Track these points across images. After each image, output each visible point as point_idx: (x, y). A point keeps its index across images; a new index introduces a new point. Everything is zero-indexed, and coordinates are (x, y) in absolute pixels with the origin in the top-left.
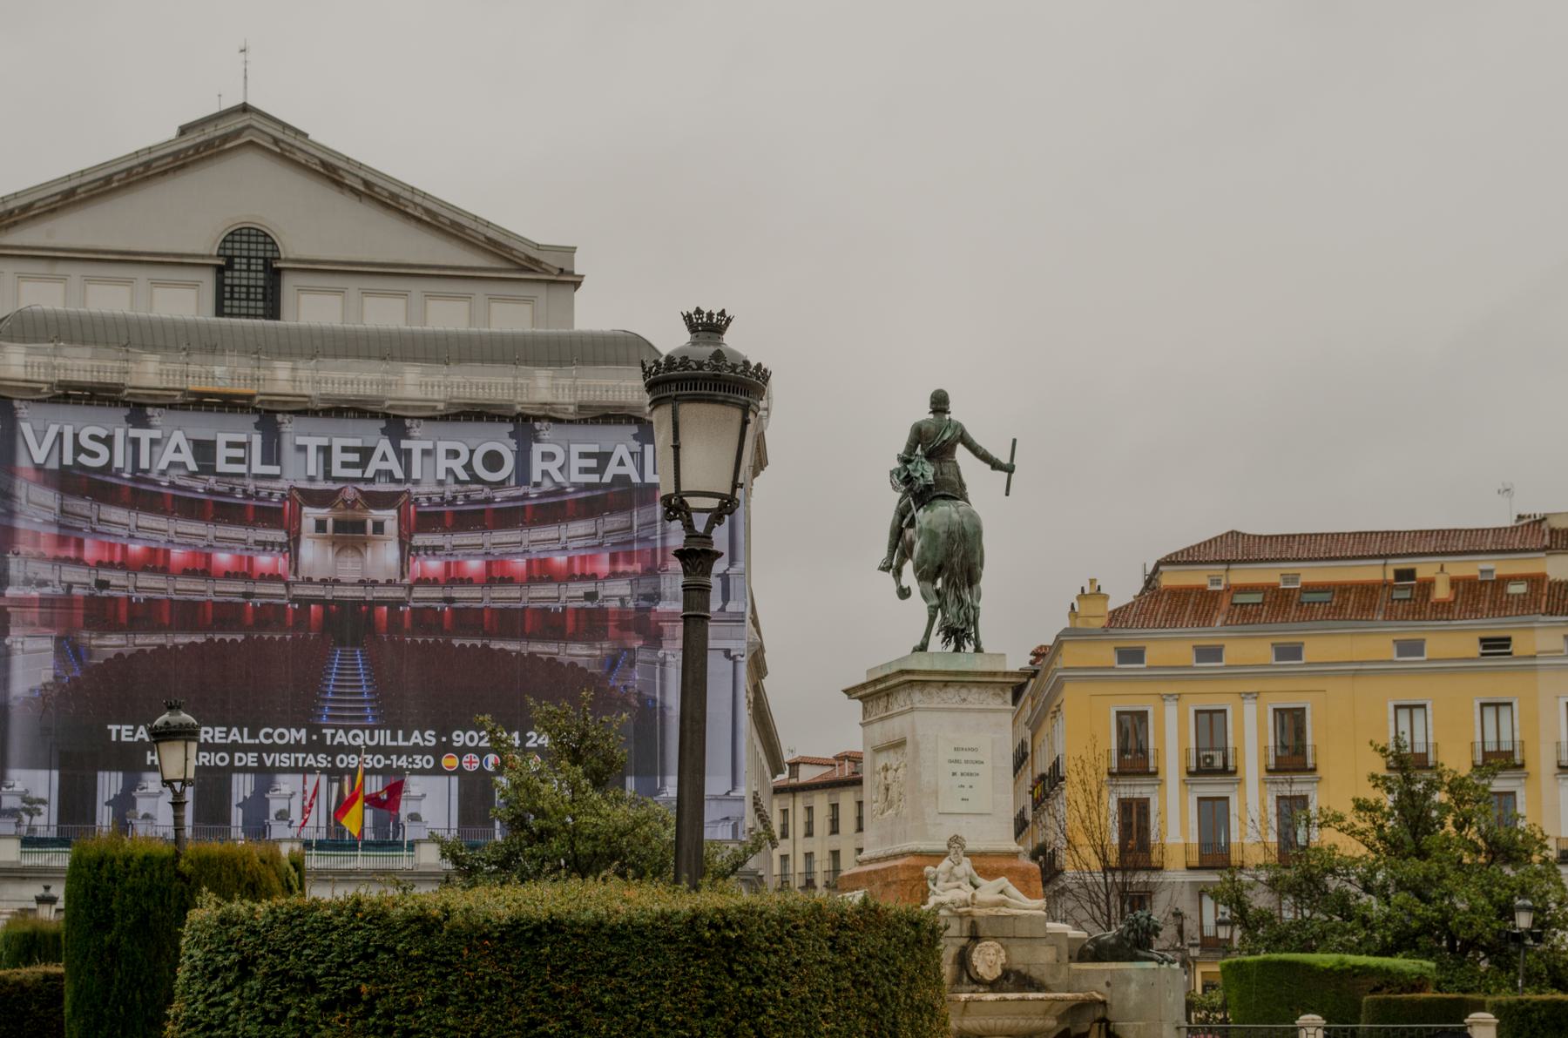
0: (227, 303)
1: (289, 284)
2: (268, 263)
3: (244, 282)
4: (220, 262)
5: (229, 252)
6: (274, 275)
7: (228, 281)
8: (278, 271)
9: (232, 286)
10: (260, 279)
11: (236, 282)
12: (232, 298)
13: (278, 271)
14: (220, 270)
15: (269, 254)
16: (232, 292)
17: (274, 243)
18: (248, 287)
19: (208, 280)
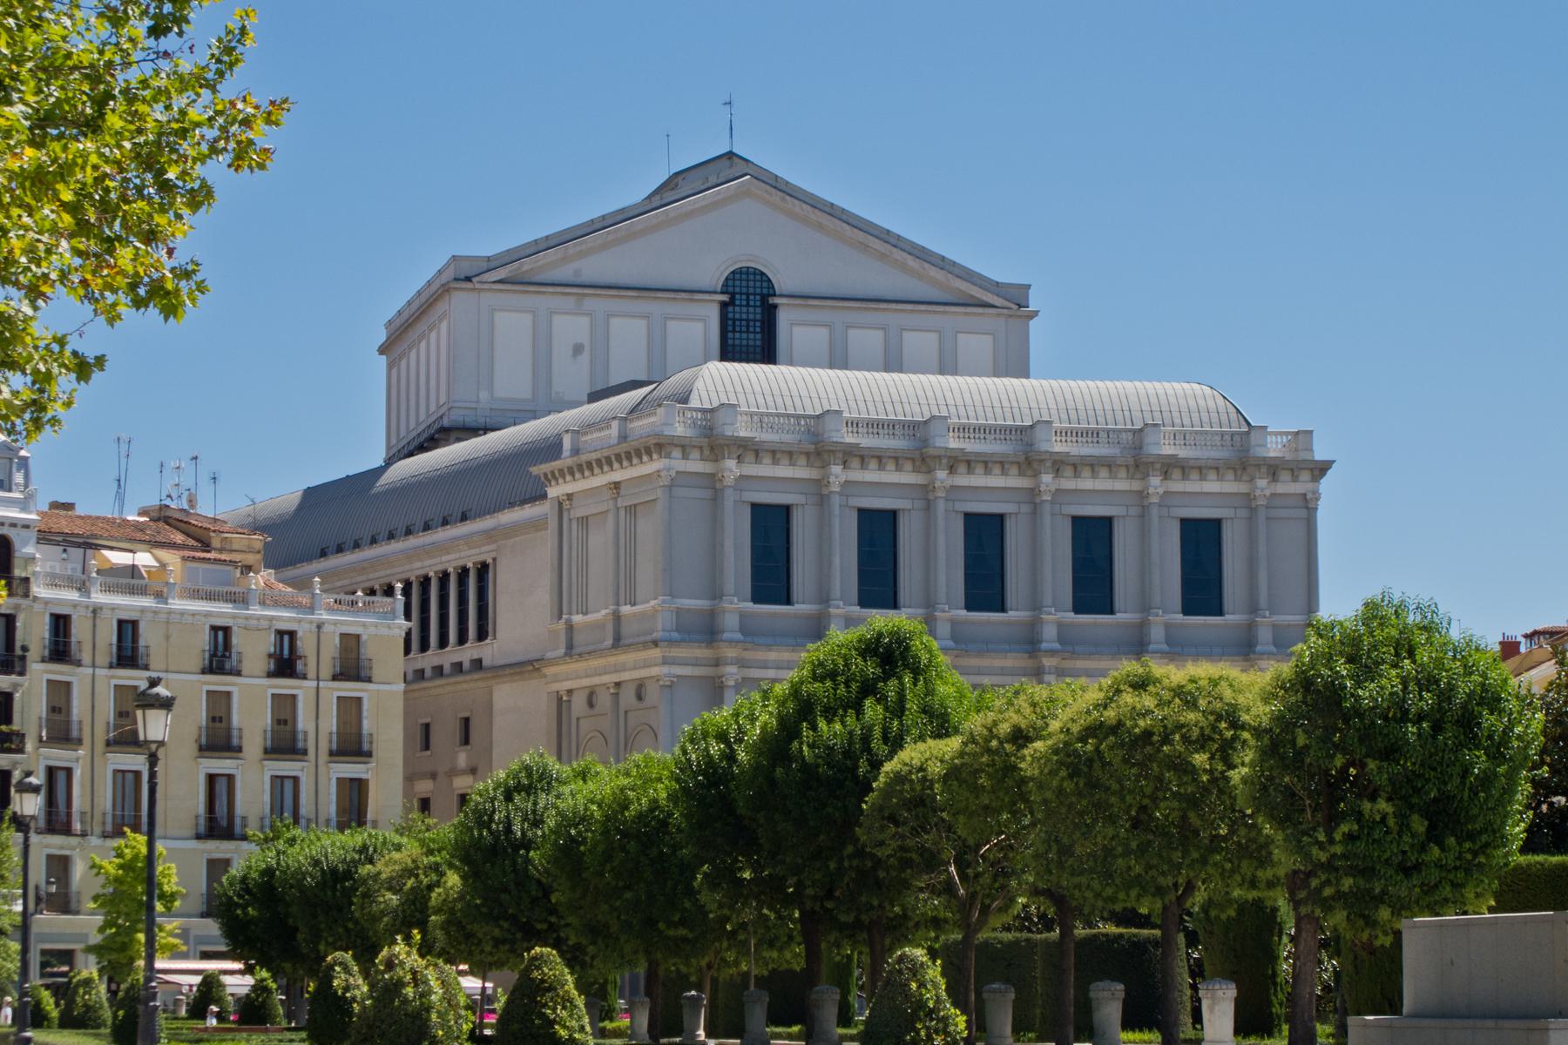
1: (784, 318)
2: (764, 298)
4: (725, 298)
6: (770, 313)
8: (775, 307)
9: (734, 320)
10: (756, 313)
12: (734, 331)
13: (775, 307)
14: (724, 305)
17: (769, 280)
19: (713, 314)
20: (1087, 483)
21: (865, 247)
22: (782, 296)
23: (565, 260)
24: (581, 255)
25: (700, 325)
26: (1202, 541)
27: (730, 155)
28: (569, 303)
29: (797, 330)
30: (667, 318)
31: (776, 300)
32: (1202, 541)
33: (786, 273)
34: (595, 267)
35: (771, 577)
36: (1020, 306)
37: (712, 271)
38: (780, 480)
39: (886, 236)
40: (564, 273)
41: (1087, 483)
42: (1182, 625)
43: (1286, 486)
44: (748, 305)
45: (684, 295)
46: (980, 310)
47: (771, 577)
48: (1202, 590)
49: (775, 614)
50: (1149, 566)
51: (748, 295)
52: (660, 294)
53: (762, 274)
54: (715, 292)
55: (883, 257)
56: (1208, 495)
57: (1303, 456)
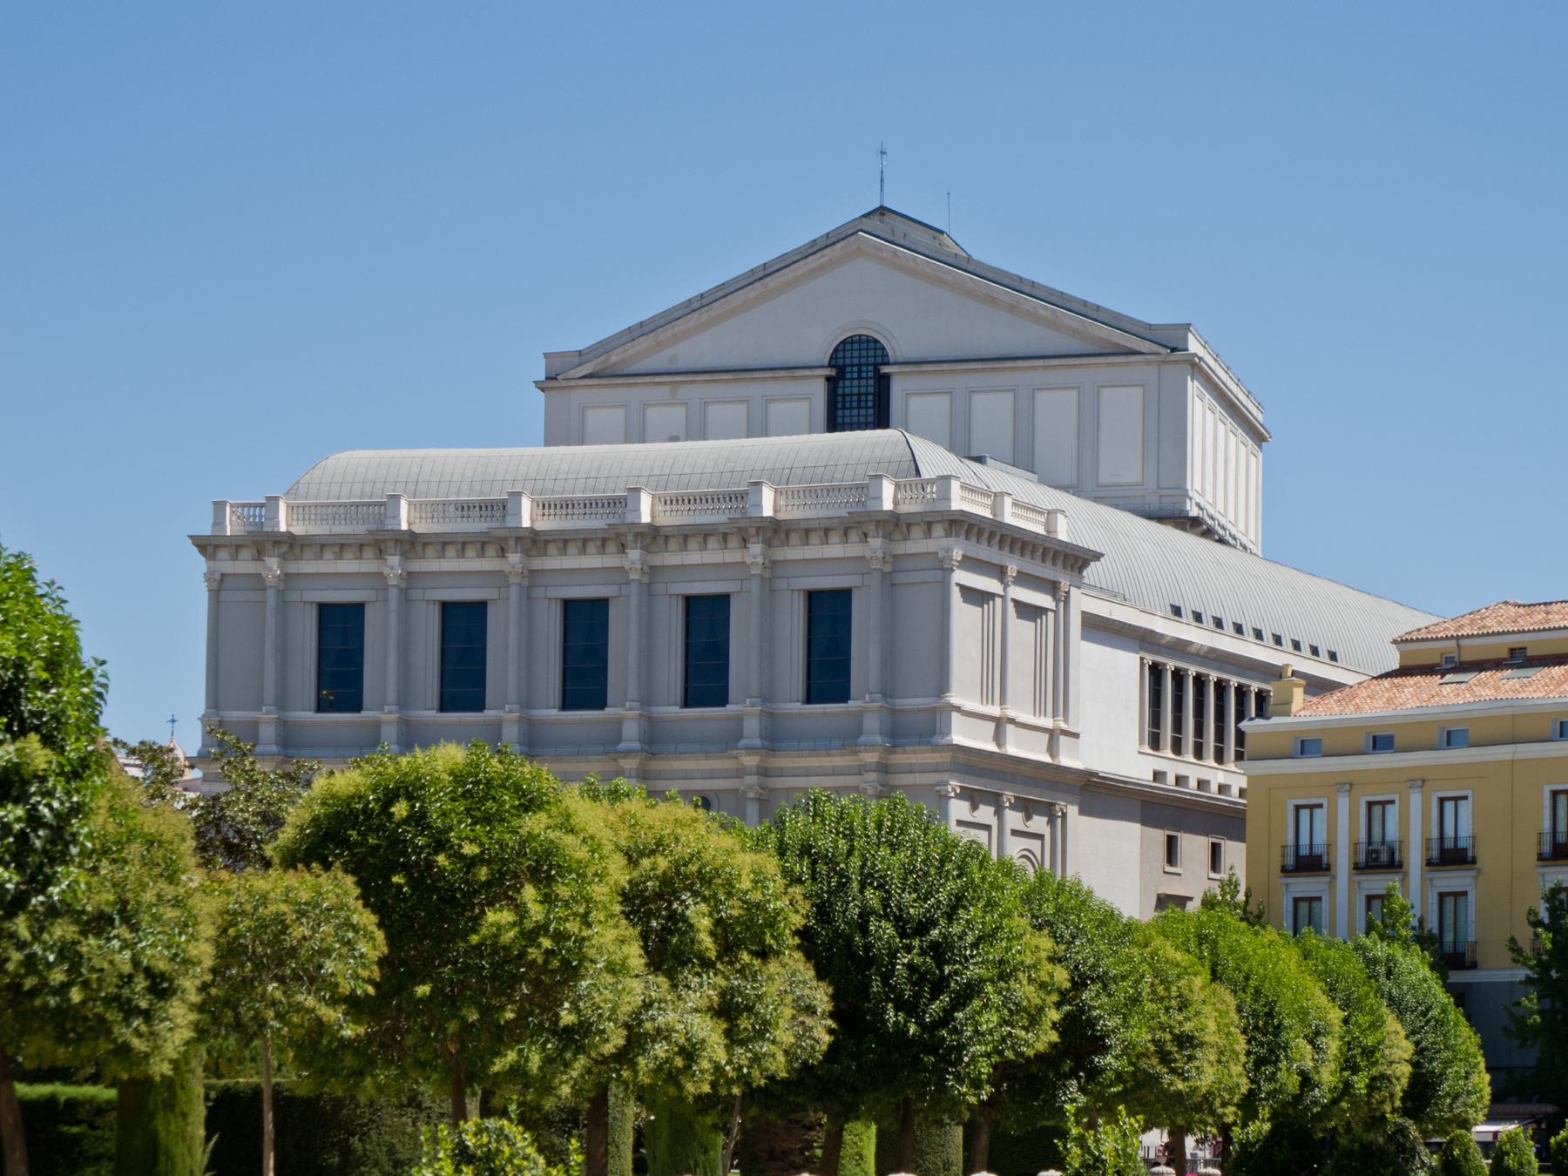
0: (840, 413)
1: (897, 389)
3: (855, 390)
4: (833, 372)
5: (840, 362)
6: (883, 384)
7: (840, 391)
8: (887, 377)
9: (844, 396)
11: (847, 391)
12: (844, 408)
13: (887, 377)
14: (828, 379)
15: (879, 360)
16: (844, 402)
17: (883, 348)
18: (859, 395)
20: (694, 557)
21: (991, 300)
22: (896, 363)
23: (660, 346)
24: (677, 339)
25: (805, 405)
26: (828, 615)
27: (882, 211)
28: (662, 393)
29: (915, 402)
30: (768, 401)
31: (885, 369)
32: (828, 615)
33: (900, 342)
34: (691, 352)
35: (340, 681)
36: (1173, 350)
37: (817, 344)
38: (339, 577)
39: (1016, 284)
40: (658, 361)
41: (694, 557)
42: (800, 715)
43: (917, 545)
44: (860, 378)
45: (782, 373)
46: (1123, 359)
47: (340, 681)
48: (828, 675)
49: (338, 723)
50: (767, 648)
51: (859, 366)
52: (756, 375)
53: (876, 341)
54: (822, 367)
55: (1013, 308)
56: (828, 562)
57: (941, 507)
